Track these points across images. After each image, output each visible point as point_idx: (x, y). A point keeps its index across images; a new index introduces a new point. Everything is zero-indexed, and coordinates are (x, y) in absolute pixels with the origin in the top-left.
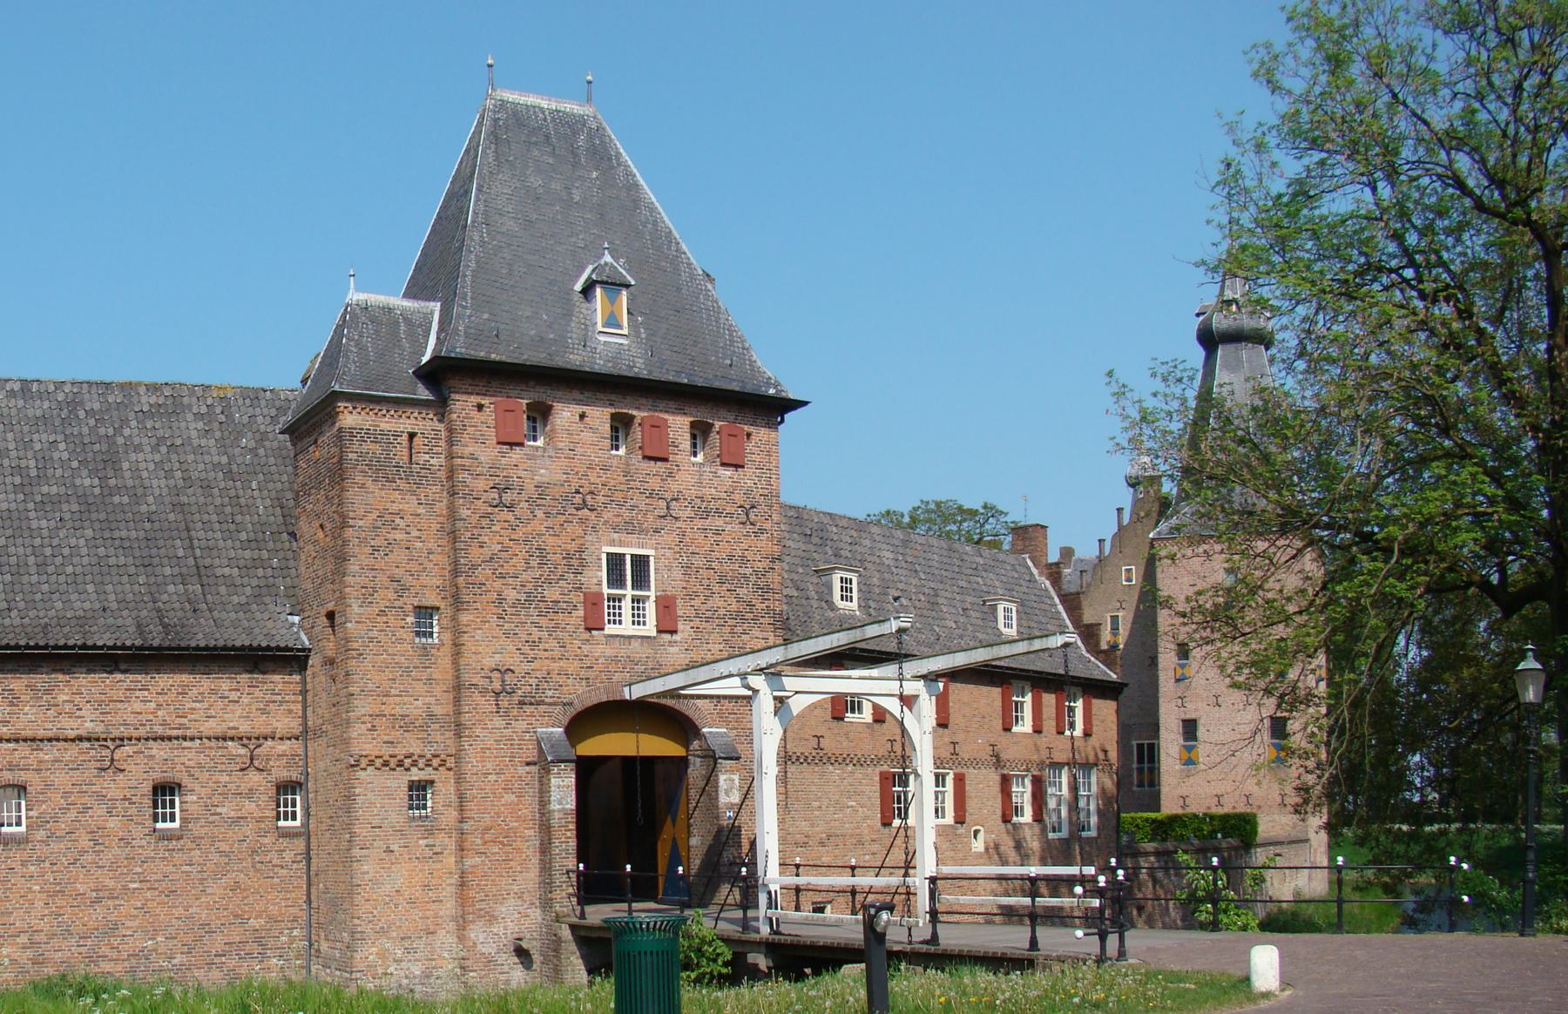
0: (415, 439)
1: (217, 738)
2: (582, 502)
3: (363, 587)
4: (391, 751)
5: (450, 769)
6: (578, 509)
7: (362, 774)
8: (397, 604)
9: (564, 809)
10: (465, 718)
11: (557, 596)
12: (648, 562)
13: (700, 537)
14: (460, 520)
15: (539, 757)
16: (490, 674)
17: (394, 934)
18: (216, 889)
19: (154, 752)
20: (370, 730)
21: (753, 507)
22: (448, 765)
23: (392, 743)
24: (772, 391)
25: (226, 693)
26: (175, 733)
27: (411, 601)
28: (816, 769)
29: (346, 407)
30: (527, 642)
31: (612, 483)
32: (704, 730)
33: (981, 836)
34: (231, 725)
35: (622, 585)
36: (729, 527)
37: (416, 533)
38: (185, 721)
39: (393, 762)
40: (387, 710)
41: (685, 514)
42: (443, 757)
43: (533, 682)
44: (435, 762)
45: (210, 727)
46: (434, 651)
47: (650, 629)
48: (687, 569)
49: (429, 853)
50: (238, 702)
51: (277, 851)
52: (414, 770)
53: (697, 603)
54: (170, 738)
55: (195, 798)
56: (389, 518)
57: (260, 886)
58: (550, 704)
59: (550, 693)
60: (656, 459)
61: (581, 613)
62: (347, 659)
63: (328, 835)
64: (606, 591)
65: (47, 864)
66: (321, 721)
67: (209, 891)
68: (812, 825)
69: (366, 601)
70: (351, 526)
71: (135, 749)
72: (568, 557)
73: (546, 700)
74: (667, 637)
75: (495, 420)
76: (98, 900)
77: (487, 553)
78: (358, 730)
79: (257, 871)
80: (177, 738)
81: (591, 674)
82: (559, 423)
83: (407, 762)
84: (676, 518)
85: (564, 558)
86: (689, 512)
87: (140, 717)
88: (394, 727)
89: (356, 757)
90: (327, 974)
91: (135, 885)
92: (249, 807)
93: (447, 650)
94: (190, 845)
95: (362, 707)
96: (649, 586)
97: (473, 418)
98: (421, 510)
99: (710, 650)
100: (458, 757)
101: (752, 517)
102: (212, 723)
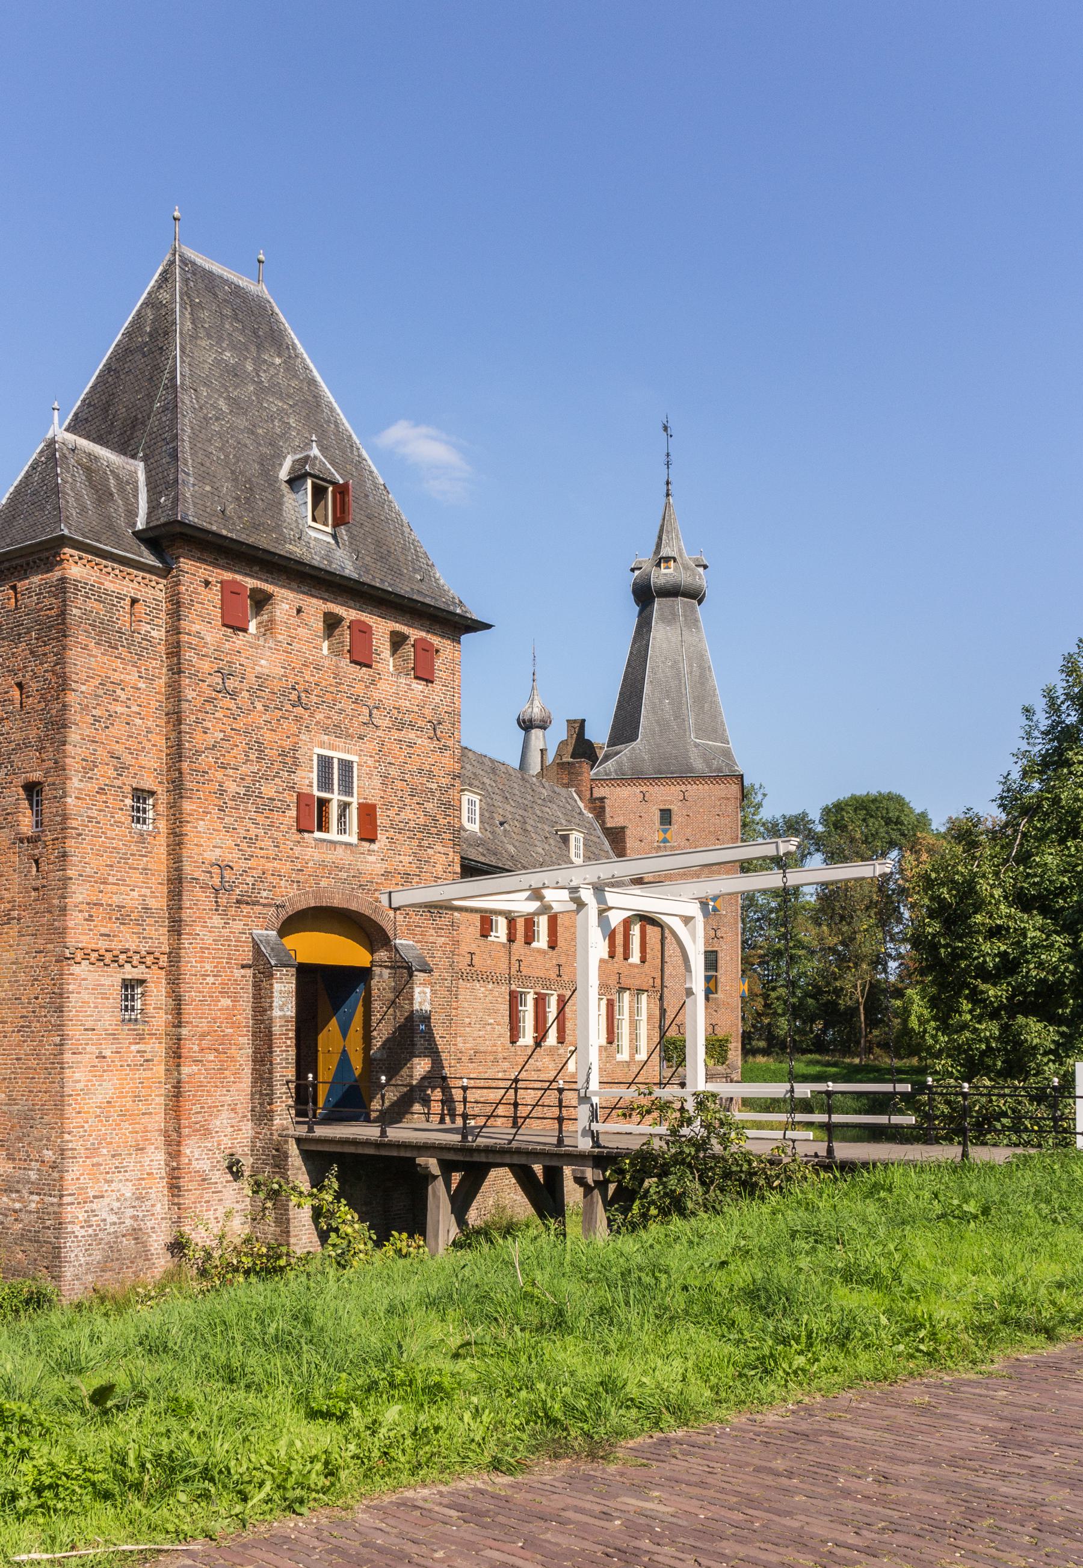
0: (136, 606)
3: (83, 760)
5: (161, 968)
7: (76, 969)
9: (284, 1016)
10: (186, 914)
11: (272, 794)
12: (332, 764)
14: (187, 701)
15: (254, 959)
17: (105, 1151)
22: (161, 964)
23: (108, 936)
24: (458, 611)
29: (71, 556)
30: (245, 838)
31: (324, 683)
32: (398, 941)
36: (419, 741)
39: (108, 956)
42: (157, 954)
43: (250, 880)
44: (149, 960)
52: (128, 966)
53: (390, 813)
56: (108, 685)
58: (264, 905)
59: (264, 894)
61: (294, 813)
62: (65, 838)
63: (16, 1037)
66: (9, 906)
73: (262, 901)
74: (366, 844)
75: (222, 600)
78: (75, 920)
81: (301, 878)
82: (278, 614)
83: (123, 957)
85: (280, 755)
88: (110, 918)
89: (72, 950)
90: (14, 1200)
93: (162, 840)
95: (79, 894)
97: (200, 594)
98: (142, 685)
100: (175, 956)
101: (438, 733)
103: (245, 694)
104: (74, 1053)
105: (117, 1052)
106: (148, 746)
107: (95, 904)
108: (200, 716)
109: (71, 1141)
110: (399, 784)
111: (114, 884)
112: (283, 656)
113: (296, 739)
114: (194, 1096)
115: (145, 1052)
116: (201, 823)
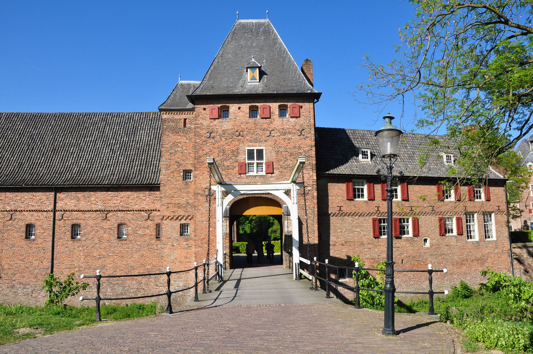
1: (138, 211)
2: (239, 134)
4: (174, 214)
7: (165, 222)
13: (282, 142)
18: (136, 256)
19: (119, 215)
21: (303, 130)
24: (309, 92)
25: (142, 198)
26: (125, 209)
27: (182, 168)
28: (340, 218)
31: (250, 127)
33: (428, 241)
35: (253, 159)
37: (186, 148)
38: (128, 206)
41: (276, 135)
45: (137, 207)
46: (190, 183)
47: (264, 173)
48: (277, 152)
49: (186, 246)
53: (281, 163)
54: (124, 211)
55: (130, 228)
60: (266, 118)
61: (237, 169)
64: (247, 161)
65: (85, 247)
67: (134, 256)
68: (338, 238)
69: (167, 169)
71: (113, 214)
72: (233, 151)
74: (270, 175)
76: (100, 258)
77: (205, 152)
80: (126, 211)
86: (278, 134)
87: (115, 205)
91: (111, 254)
92: (148, 231)
94: (128, 243)
96: (263, 159)
102: (137, 206)
106: (189, 157)
112: (233, 122)
113: (238, 146)
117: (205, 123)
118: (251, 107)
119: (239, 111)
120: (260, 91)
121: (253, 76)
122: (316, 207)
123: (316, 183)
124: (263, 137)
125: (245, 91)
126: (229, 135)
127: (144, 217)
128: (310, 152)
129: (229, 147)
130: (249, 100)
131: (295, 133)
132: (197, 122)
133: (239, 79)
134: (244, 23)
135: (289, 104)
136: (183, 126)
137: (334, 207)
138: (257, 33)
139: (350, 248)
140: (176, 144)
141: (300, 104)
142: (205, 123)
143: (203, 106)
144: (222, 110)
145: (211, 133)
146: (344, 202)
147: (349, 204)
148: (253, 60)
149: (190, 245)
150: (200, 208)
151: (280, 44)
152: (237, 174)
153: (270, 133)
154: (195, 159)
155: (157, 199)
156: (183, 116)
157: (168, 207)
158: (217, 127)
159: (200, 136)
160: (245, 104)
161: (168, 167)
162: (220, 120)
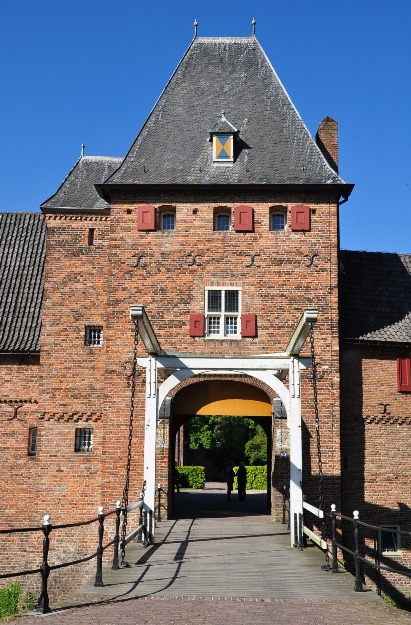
3: (53, 315)
4: (65, 410)
6: (189, 265)
7: (46, 424)
8: (75, 324)
13: (275, 277)
16: (125, 365)
20: (52, 397)
21: (315, 255)
23: (66, 405)
24: (329, 182)
28: (384, 427)
31: (214, 248)
34: (5, 394)
35: (219, 308)
36: (297, 269)
37: (91, 284)
40: (63, 385)
46: (97, 352)
47: (238, 336)
48: (265, 298)
49: (86, 473)
50: (10, 381)
51: (26, 468)
53: (271, 318)
57: (14, 489)
60: (245, 232)
61: (188, 327)
69: (55, 322)
70: (49, 282)
72: (181, 293)
74: (249, 340)
77: (127, 293)
79: (12, 480)
84: (258, 266)
86: (268, 262)
92: (12, 442)
99: (281, 348)
103: (153, 265)
104: (43, 469)
105: (71, 468)
106: (97, 302)
107: (57, 389)
108: (121, 282)
109: (37, 517)
110: (279, 299)
111: (70, 377)
114: (110, 494)
115: (90, 468)
116: (120, 339)
117: (130, 238)
118: (216, 211)
119: (194, 216)
120: (235, 180)
121: (223, 151)
122: (338, 404)
123: (337, 358)
124: (239, 267)
125: (207, 180)
126: (175, 263)
127: (8, 414)
128: (328, 298)
129: (174, 285)
130: (214, 196)
131: (299, 262)
132: (114, 236)
133: (196, 156)
134: (208, 44)
135: (290, 206)
136: (87, 243)
137: (372, 404)
138: (233, 66)
139: (405, 488)
140: (73, 276)
141: (312, 206)
142: (130, 238)
143: (126, 206)
144: (163, 214)
145: (140, 257)
146: (394, 396)
147: (403, 401)
148: (224, 119)
149: (92, 471)
150: (115, 399)
151: (277, 87)
152: (188, 337)
153: (253, 260)
154: (109, 306)
155: (33, 379)
156: (88, 224)
157: (54, 396)
158: (153, 247)
159: (119, 262)
160: (207, 205)
161: (56, 320)
162: (158, 233)
